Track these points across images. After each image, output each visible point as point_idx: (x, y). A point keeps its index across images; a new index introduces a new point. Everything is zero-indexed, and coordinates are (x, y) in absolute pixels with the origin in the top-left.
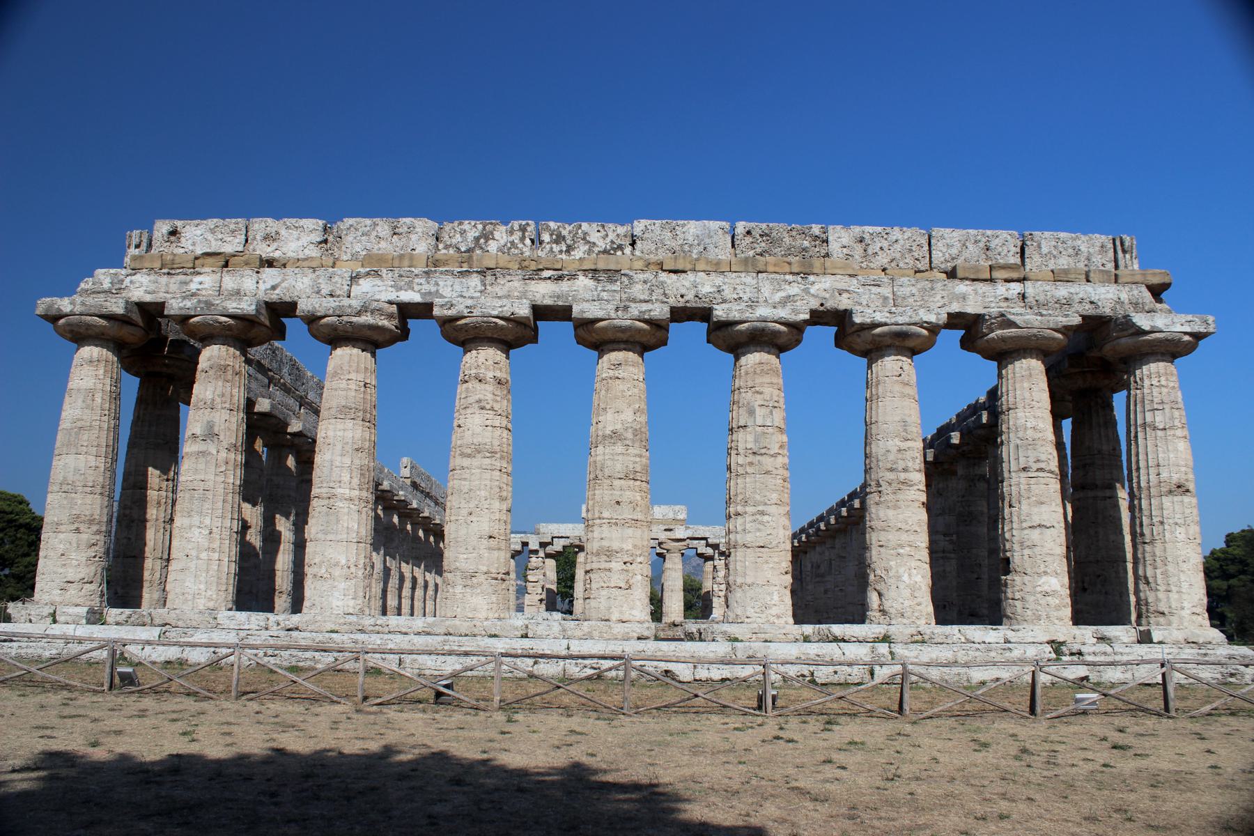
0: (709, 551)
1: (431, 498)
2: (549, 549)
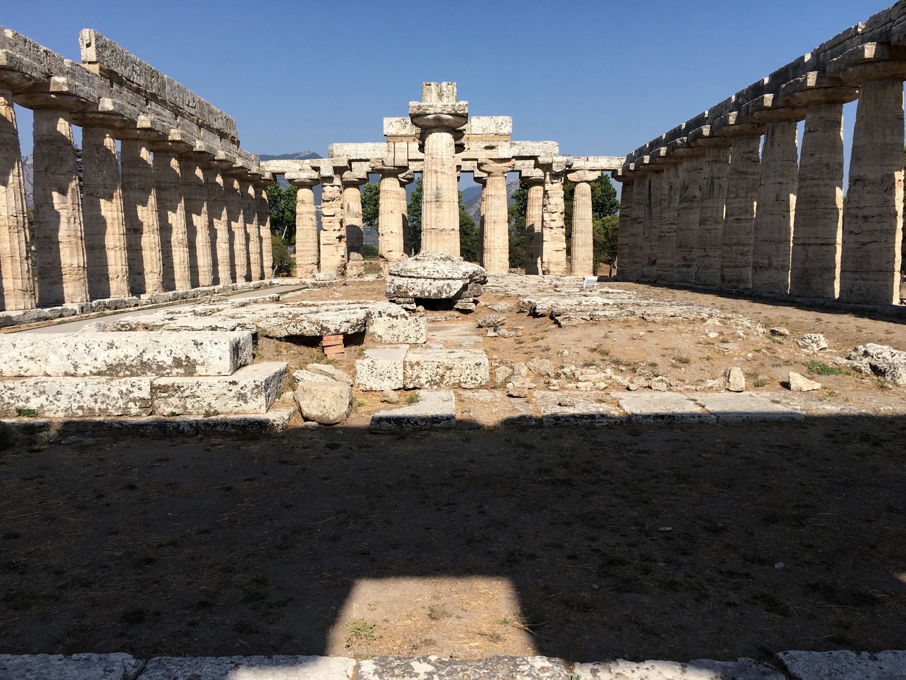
0: (538, 173)
1: (163, 103)
2: (347, 175)
